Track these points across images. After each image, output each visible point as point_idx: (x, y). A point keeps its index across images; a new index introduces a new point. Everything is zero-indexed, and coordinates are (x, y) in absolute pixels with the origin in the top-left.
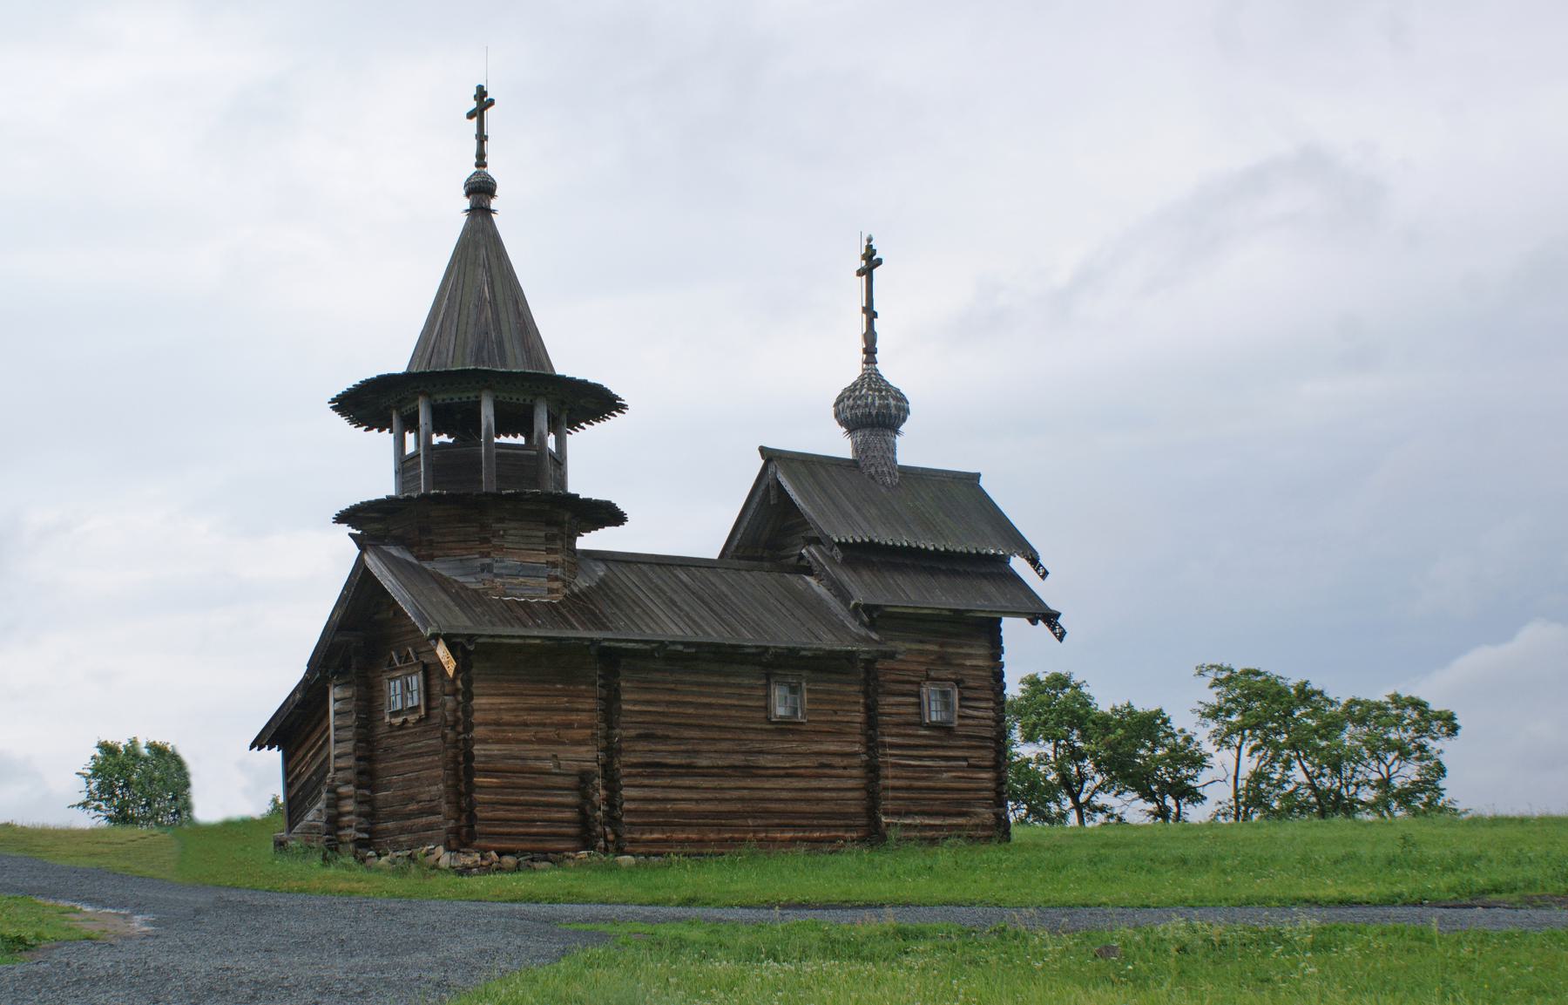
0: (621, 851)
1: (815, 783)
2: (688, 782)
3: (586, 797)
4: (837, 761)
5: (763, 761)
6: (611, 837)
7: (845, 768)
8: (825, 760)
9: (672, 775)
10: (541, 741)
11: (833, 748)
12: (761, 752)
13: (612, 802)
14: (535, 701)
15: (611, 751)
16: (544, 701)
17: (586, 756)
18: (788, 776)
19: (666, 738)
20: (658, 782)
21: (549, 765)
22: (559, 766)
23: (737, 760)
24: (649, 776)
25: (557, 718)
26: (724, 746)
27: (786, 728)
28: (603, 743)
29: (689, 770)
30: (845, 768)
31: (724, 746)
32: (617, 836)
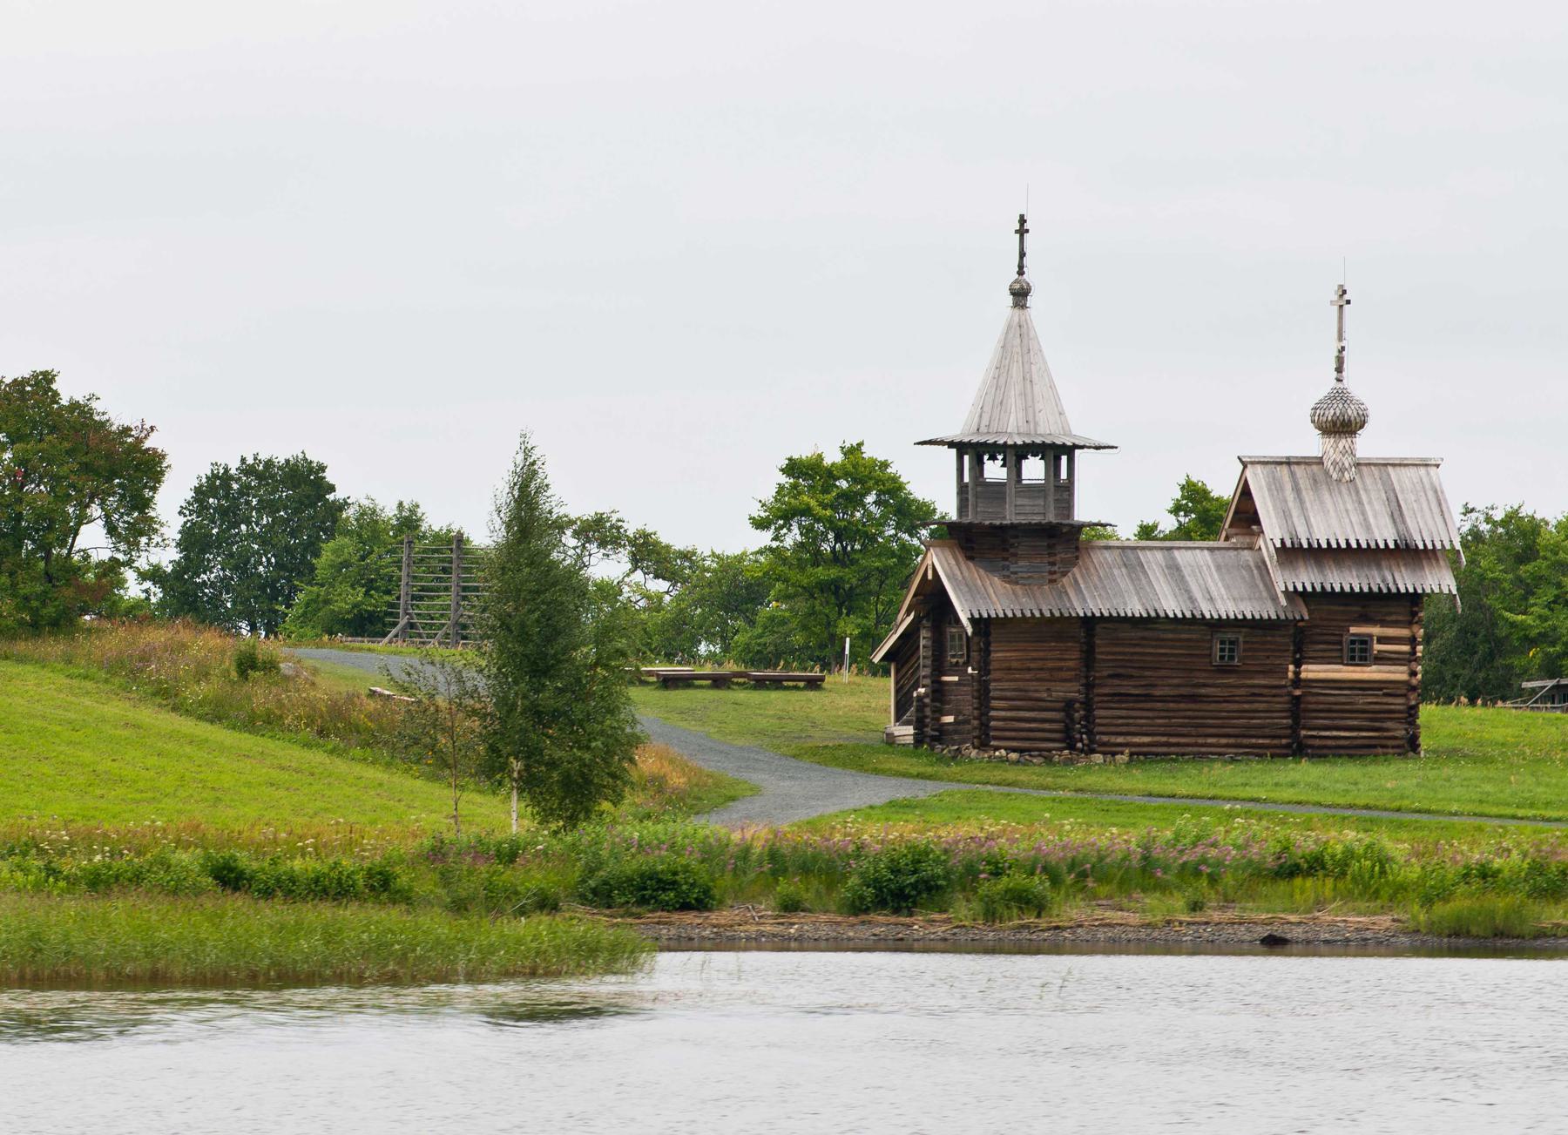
0: (1093, 751)
1: (1246, 706)
2: (1149, 705)
3: (1070, 716)
5: (1203, 691)
10: (1038, 680)
12: (1205, 685)
13: (1089, 718)
14: (1035, 654)
15: (1089, 687)
16: (1041, 654)
17: (1073, 691)
21: (1045, 695)
23: (1184, 691)
25: (1050, 664)
29: (1148, 698)
31: (1176, 681)
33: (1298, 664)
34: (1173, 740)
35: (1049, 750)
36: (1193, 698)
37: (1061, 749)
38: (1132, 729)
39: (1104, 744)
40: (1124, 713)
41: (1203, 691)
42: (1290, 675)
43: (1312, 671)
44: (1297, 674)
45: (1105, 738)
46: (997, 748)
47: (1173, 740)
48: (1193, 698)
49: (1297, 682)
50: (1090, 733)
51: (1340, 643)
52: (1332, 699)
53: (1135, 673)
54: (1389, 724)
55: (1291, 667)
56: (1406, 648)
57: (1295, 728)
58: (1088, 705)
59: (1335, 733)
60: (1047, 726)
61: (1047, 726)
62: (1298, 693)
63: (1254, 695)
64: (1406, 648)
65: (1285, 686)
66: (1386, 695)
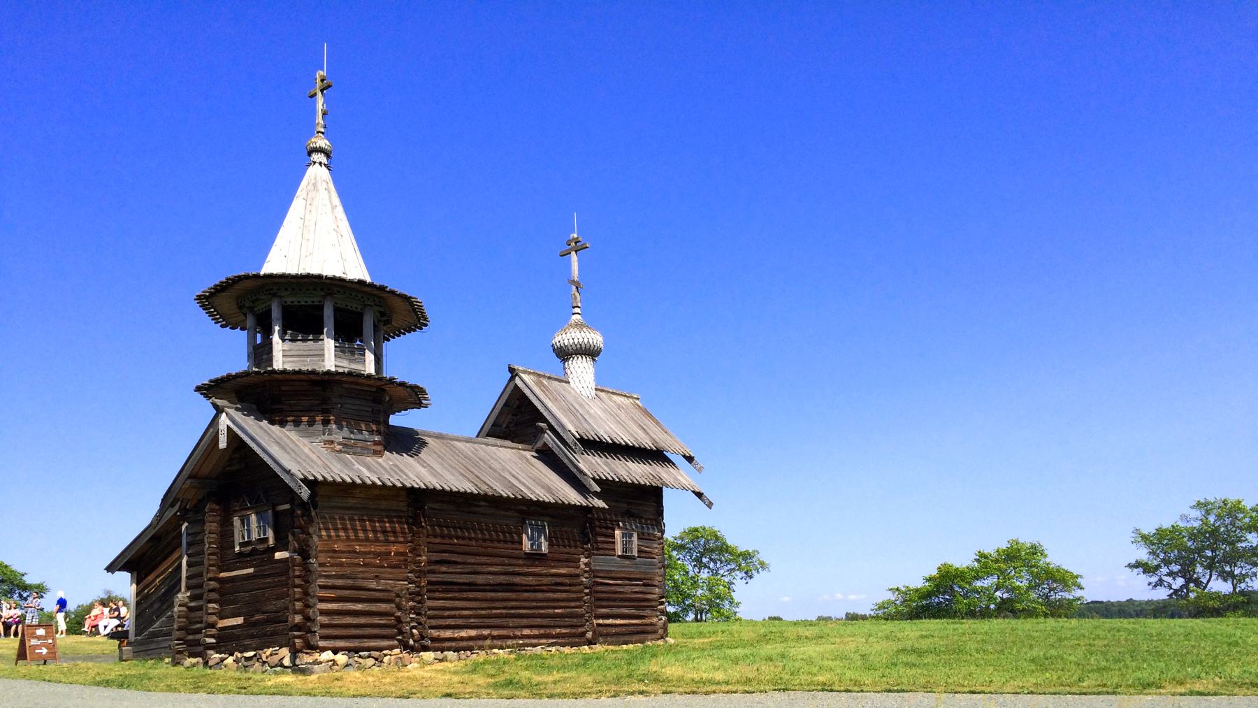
2: (471, 595)
4: (567, 581)
5: (517, 580)
8: (559, 580)
9: (460, 591)
11: (563, 571)
18: (535, 591)
21: (373, 585)
23: (502, 579)
24: (444, 591)
27: (535, 557)
35: (380, 649)
37: (391, 648)
38: (460, 622)
39: (433, 640)
45: (435, 633)
46: (323, 650)
47: (495, 633)
52: (613, 588)
53: (459, 559)
60: (376, 620)
61: (376, 620)
63: (557, 584)
65: (578, 576)
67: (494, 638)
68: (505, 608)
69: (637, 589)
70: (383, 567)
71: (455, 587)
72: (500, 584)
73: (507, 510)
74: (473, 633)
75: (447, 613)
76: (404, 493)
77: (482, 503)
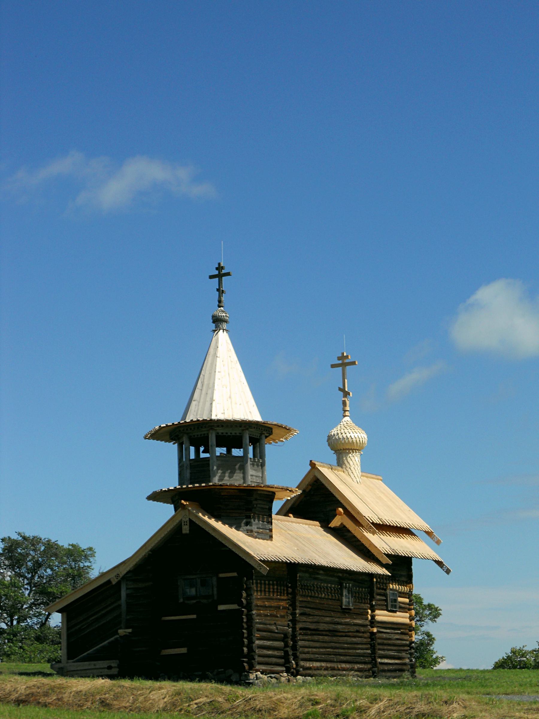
1: (354, 639)
2: (316, 638)
5: (339, 627)
6: (294, 666)
7: (363, 633)
9: (312, 635)
10: (271, 615)
12: (338, 624)
19: (309, 615)
20: (306, 638)
21: (273, 627)
22: (277, 629)
23: (332, 627)
26: (328, 619)
27: (346, 612)
28: (291, 617)
29: (316, 632)
30: (363, 633)
31: (328, 619)
32: (297, 664)
33: (373, 611)
34: (329, 665)
36: (333, 633)
38: (312, 656)
40: (307, 643)
41: (339, 627)
42: (370, 617)
43: (382, 616)
44: (373, 617)
48: (333, 633)
49: (373, 622)
50: (296, 658)
51: (385, 595)
52: (384, 636)
54: (403, 654)
55: (369, 611)
56: (407, 600)
57: (373, 656)
58: (294, 637)
59: (386, 661)
62: (375, 630)
63: (358, 631)
64: (407, 600)
66: (402, 633)
67: (326, 669)
68: (332, 648)
69: (397, 637)
70: (278, 617)
71: (309, 632)
72: (329, 631)
73: (333, 576)
74: (317, 664)
75: (306, 650)
76: (285, 565)
77: (321, 572)
